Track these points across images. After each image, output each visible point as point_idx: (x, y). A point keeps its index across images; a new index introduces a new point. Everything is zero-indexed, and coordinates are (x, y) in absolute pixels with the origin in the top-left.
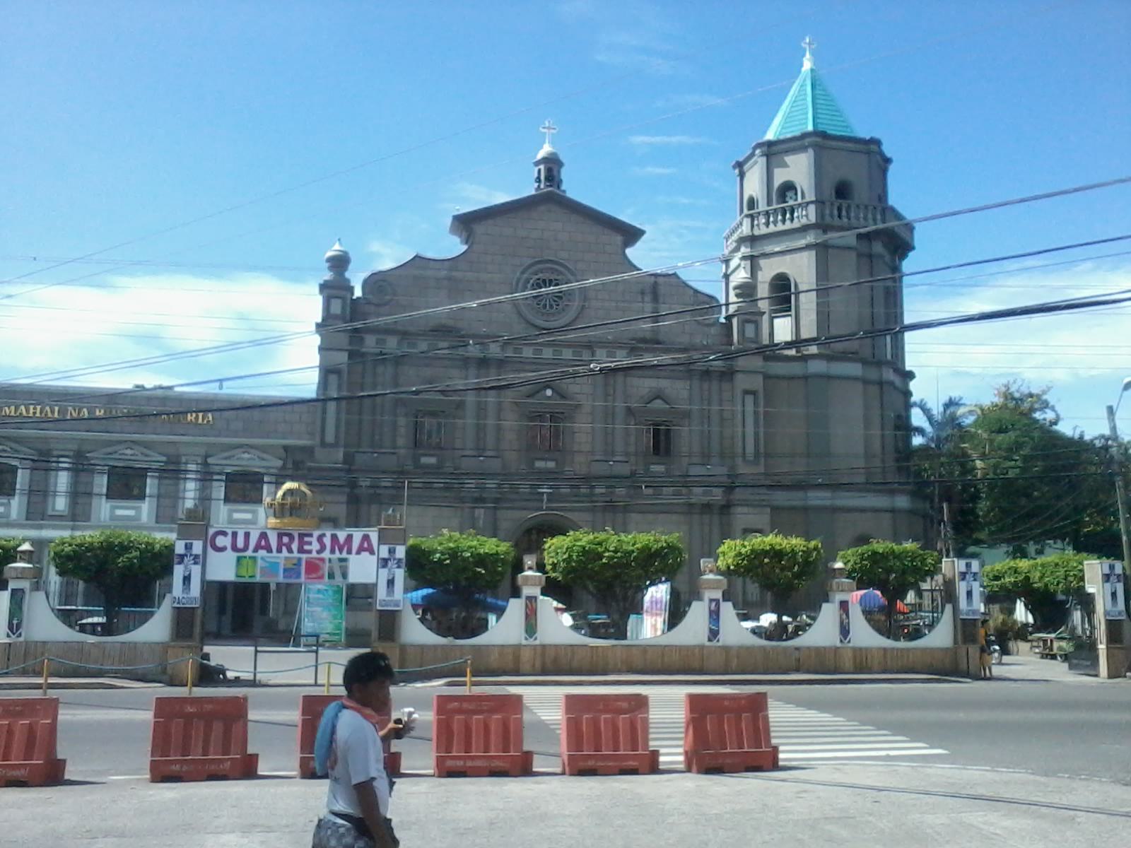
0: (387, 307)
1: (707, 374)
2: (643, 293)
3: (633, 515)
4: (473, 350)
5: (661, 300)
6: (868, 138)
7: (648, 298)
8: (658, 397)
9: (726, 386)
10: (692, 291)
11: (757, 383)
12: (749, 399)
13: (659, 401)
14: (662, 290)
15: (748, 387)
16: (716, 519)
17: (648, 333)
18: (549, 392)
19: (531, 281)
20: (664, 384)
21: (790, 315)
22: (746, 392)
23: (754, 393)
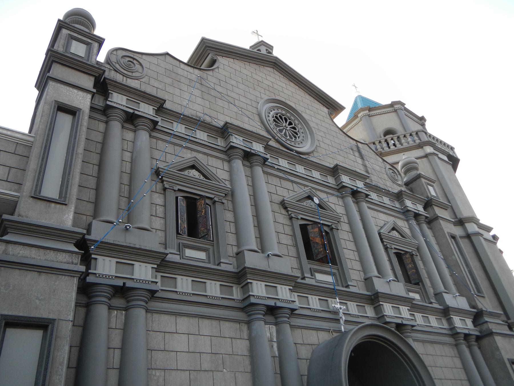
8: (193, 167)
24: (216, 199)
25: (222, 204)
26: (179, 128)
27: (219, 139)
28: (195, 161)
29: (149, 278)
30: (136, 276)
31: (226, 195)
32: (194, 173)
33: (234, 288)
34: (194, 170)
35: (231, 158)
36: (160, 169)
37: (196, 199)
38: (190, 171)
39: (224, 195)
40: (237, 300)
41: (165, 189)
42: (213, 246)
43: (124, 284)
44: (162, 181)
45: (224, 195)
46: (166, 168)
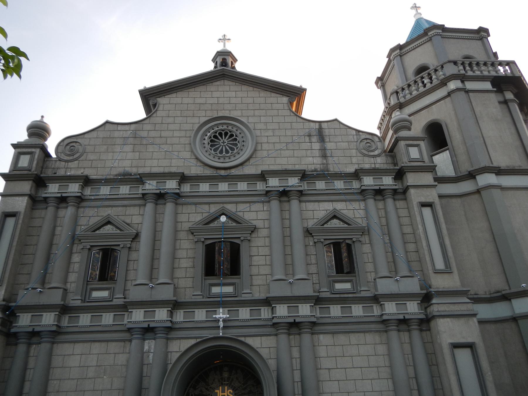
0: (76, 162)
1: (379, 193)
2: (310, 136)
3: (321, 337)
4: (151, 186)
5: (327, 140)
6: (476, 28)
7: (314, 139)
8: (335, 217)
9: (401, 204)
10: (354, 132)
11: (431, 196)
12: (427, 211)
13: (335, 221)
14: (326, 132)
15: (423, 200)
16: (416, 334)
17: (319, 166)
18: (223, 219)
19: (209, 134)
20: (339, 206)
21: (448, 149)
22: (424, 205)
23: (429, 205)
24: (354, 240)
25: (359, 242)
26: (321, 185)
27: (353, 182)
28: (335, 212)
29: (309, 313)
30: (301, 313)
31: (363, 233)
32: (335, 223)
33: (375, 308)
34: (335, 220)
35: (365, 197)
36: (309, 229)
37: (340, 242)
38: (332, 221)
39: (361, 233)
40: (377, 316)
41: (315, 243)
42: (356, 276)
43: (295, 320)
44: (313, 236)
45: (361, 233)
46: (314, 227)
